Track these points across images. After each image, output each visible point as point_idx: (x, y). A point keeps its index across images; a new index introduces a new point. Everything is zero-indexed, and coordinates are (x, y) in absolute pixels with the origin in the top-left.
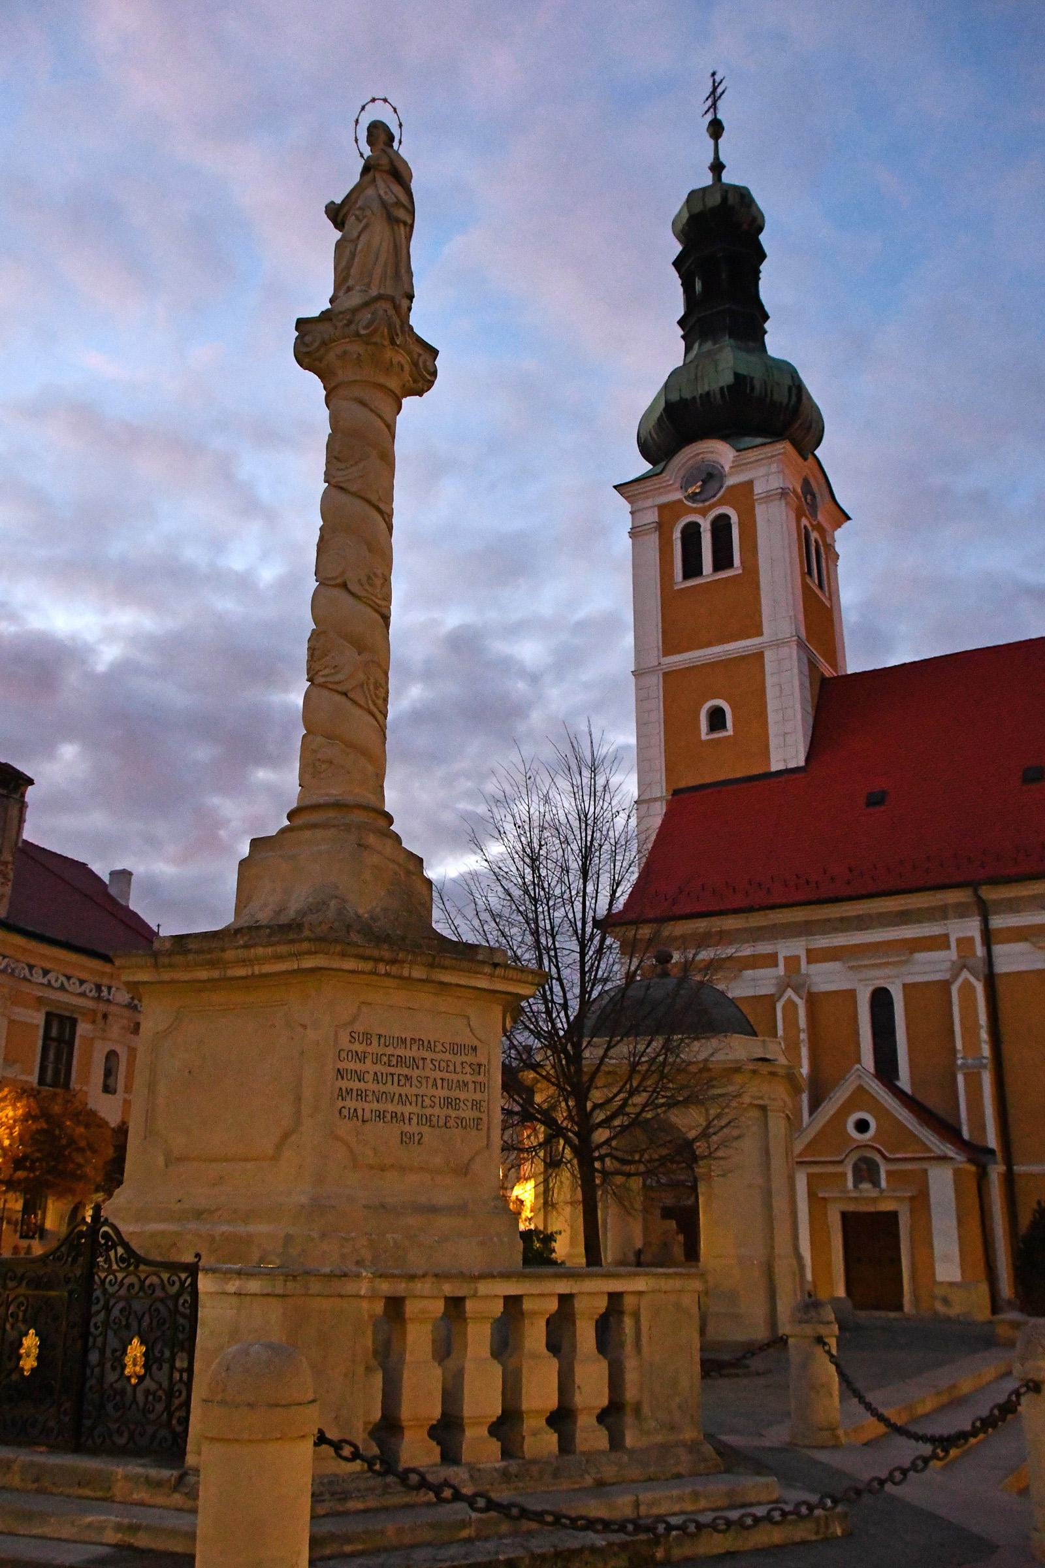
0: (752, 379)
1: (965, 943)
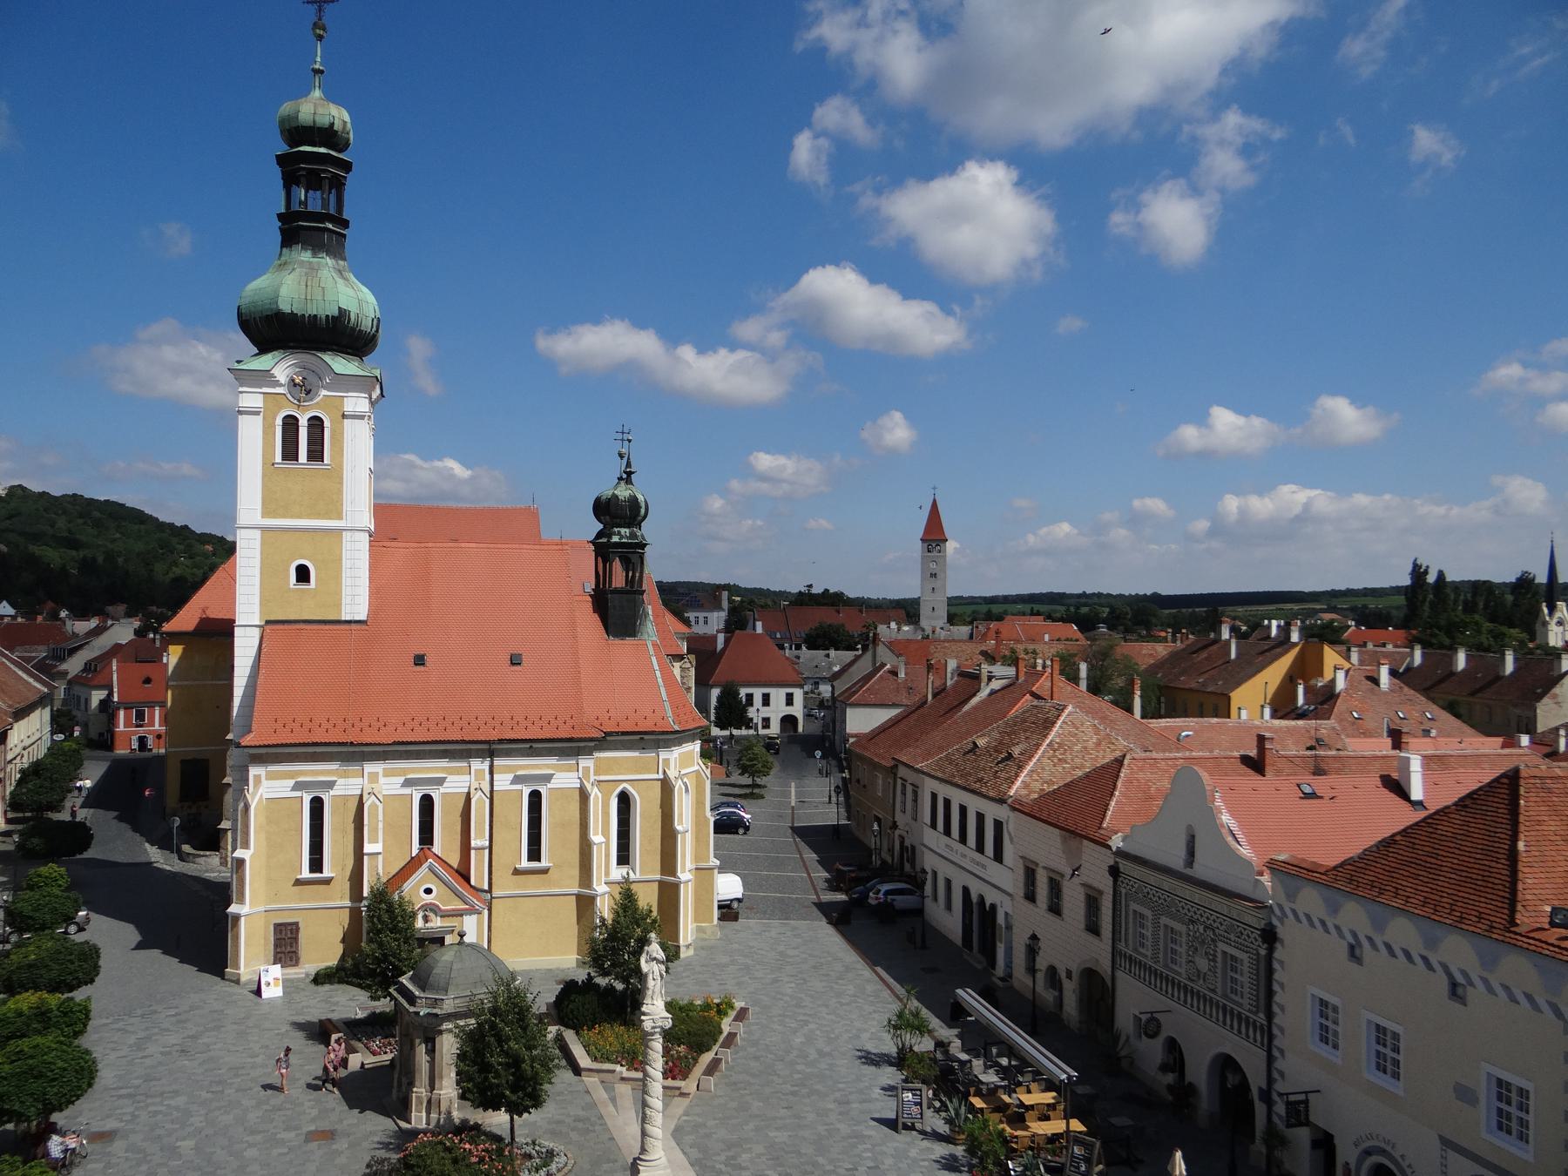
0: (349, 312)
1: (479, 772)
